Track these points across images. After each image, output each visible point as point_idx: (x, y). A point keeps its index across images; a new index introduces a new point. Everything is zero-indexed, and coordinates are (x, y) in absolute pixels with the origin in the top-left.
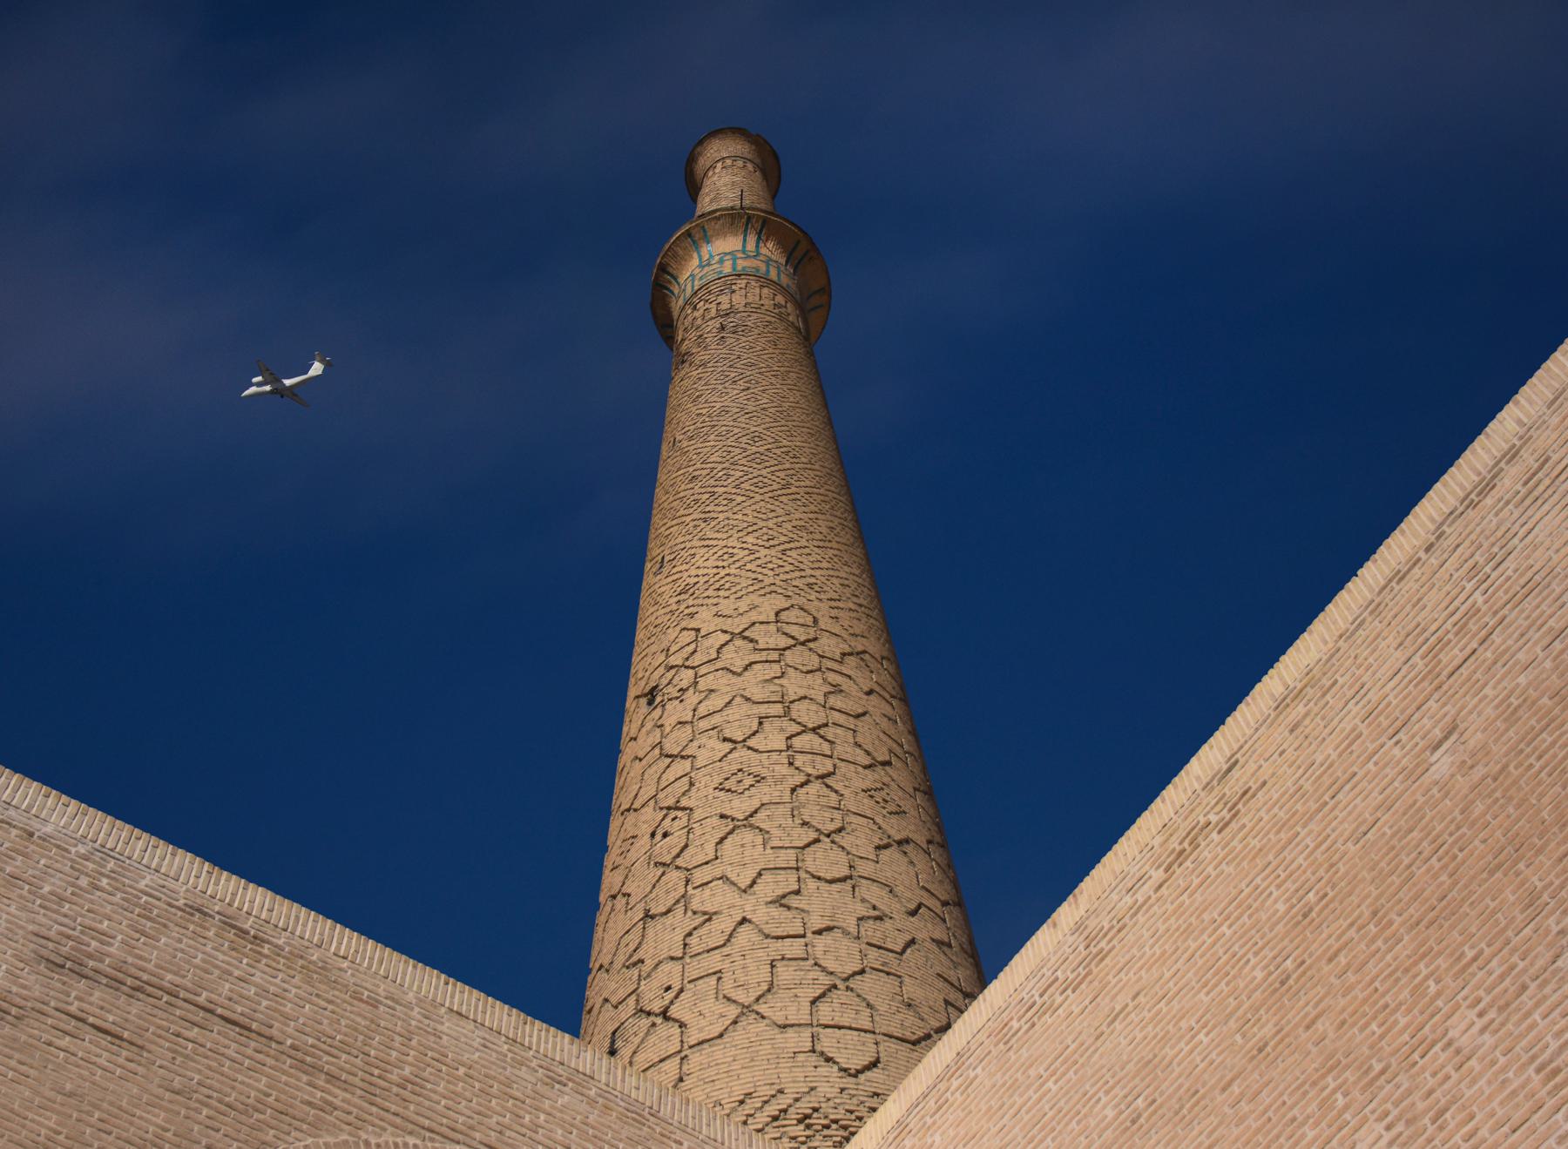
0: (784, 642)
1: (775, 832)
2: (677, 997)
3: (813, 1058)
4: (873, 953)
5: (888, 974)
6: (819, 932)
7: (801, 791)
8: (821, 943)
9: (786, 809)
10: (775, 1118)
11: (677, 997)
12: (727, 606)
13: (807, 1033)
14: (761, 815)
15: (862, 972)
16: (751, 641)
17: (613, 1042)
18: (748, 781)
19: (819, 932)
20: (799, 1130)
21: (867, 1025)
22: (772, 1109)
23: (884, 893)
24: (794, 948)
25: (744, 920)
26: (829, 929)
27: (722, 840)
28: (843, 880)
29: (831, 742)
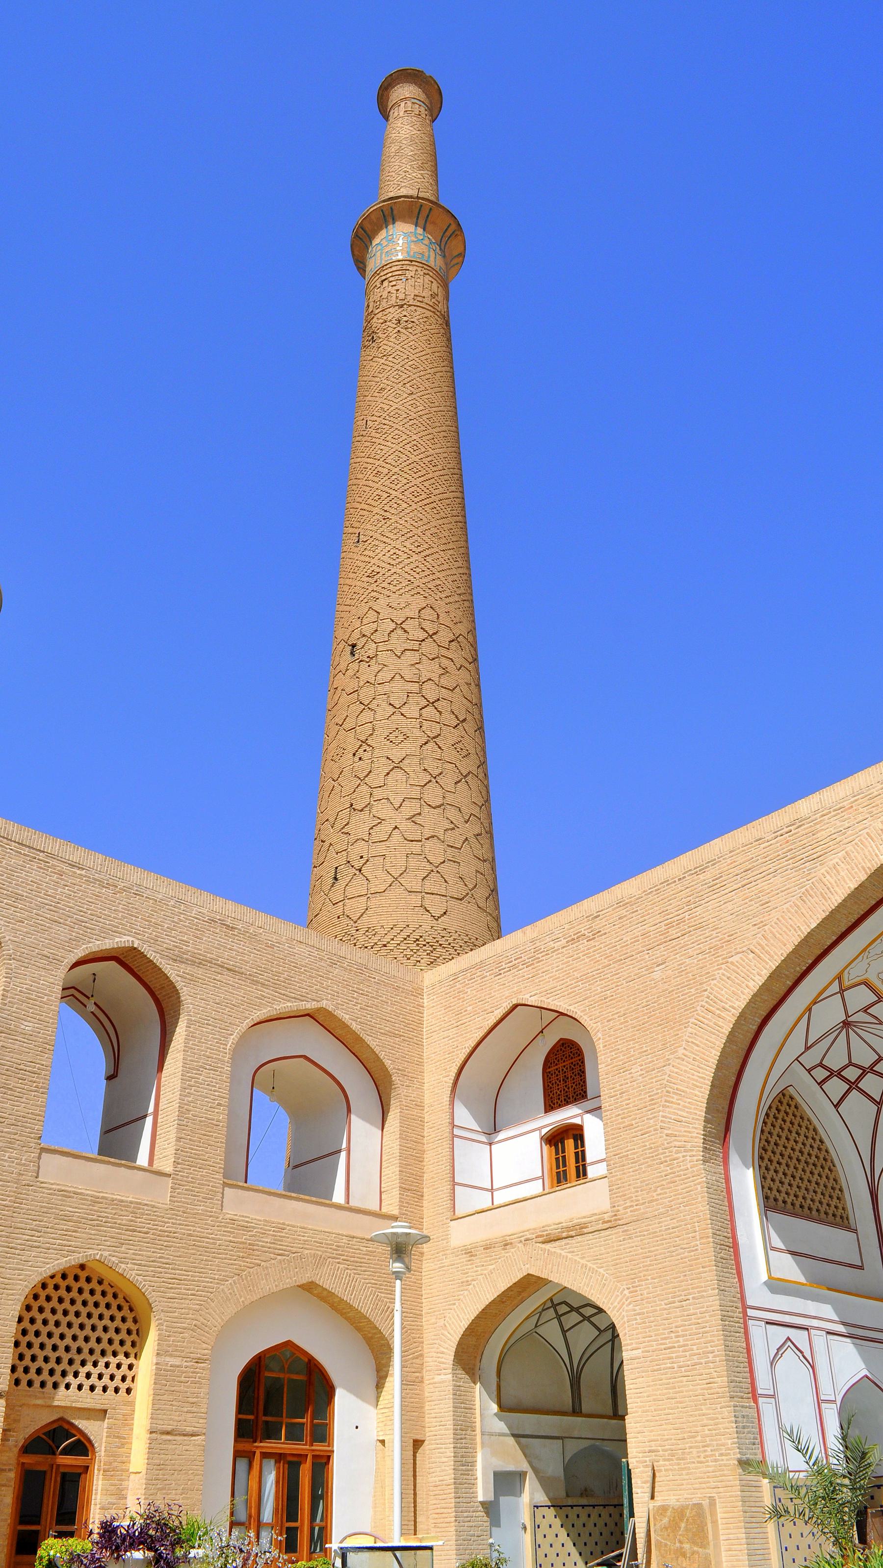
1: (412, 774)
2: (365, 863)
3: (422, 909)
4: (449, 850)
5: (454, 862)
6: (428, 839)
7: (425, 747)
8: (429, 844)
9: (416, 760)
10: (405, 939)
11: (365, 863)
12: (394, 600)
13: (419, 896)
14: (406, 762)
15: (444, 862)
17: (336, 875)
18: (401, 738)
19: (428, 839)
20: (414, 946)
21: (444, 892)
22: (404, 934)
23: (457, 812)
24: (416, 847)
25: (396, 827)
26: (433, 837)
27: (388, 774)
28: (439, 806)
29: (440, 713)
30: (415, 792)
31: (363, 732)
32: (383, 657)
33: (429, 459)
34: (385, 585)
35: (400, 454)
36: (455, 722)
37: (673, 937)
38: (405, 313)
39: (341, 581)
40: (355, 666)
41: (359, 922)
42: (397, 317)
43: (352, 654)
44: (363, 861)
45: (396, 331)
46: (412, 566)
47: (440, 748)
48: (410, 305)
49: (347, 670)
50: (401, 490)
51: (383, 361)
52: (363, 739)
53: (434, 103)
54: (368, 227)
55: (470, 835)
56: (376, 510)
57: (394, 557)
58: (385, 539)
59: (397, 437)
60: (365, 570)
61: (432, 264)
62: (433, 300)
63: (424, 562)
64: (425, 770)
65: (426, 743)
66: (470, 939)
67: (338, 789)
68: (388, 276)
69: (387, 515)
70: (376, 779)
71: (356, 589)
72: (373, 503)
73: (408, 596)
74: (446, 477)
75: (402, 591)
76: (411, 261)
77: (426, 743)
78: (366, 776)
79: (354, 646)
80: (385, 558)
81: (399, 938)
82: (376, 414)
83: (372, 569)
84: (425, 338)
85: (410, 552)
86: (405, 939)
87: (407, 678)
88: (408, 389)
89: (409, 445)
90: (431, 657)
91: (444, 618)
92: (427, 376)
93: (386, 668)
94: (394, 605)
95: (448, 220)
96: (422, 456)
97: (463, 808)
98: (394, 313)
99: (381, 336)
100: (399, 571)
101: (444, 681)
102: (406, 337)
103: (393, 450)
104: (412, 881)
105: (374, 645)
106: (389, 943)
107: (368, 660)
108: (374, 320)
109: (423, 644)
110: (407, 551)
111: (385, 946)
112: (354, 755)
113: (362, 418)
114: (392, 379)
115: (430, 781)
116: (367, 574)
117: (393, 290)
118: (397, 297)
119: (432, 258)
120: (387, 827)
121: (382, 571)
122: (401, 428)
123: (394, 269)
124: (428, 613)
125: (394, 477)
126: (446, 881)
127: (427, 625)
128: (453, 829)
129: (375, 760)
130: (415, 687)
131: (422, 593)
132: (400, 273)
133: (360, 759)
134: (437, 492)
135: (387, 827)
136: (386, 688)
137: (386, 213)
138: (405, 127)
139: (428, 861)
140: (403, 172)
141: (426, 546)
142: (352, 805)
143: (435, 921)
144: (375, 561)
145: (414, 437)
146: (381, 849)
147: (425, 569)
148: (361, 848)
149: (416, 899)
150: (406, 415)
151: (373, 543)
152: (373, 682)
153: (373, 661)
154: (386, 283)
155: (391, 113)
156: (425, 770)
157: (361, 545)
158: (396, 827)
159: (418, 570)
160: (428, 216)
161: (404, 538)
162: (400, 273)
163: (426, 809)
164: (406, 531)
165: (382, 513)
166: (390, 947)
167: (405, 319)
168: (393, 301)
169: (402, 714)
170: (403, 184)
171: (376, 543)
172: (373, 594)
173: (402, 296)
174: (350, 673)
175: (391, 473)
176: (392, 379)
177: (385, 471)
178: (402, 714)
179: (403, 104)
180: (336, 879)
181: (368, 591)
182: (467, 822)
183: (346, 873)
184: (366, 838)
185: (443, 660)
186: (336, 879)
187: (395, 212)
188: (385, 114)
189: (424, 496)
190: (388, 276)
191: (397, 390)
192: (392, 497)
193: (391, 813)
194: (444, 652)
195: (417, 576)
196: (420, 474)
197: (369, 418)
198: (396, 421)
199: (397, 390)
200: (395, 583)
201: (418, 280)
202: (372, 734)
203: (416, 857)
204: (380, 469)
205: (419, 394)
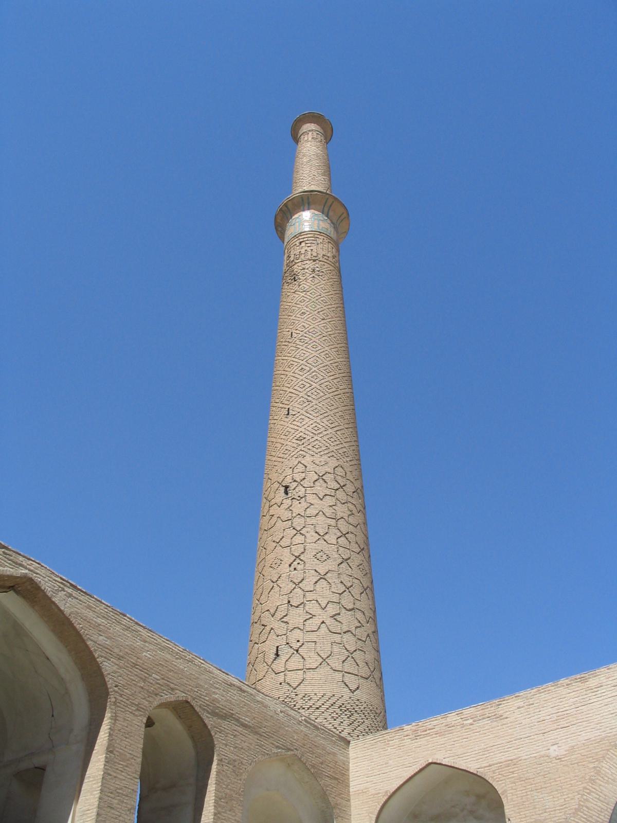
1: (333, 585)
4: (359, 642)
6: (345, 633)
8: (346, 636)
9: (335, 574)
10: (332, 705)
12: (317, 459)
16: (325, 482)
20: (338, 711)
22: (331, 701)
24: (337, 638)
25: (323, 622)
27: (316, 582)
30: (335, 598)
31: (297, 550)
32: (310, 498)
33: (336, 364)
34: (309, 447)
35: (317, 359)
36: (358, 550)
37: (564, 726)
39: (269, 439)
40: (289, 502)
41: (297, 689)
43: (286, 493)
44: (299, 644)
45: (311, 276)
47: (350, 567)
48: (320, 261)
49: (282, 503)
50: (319, 383)
51: (303, 295)
52: (297, 554)
53: (328, 134)
54: (290, 206)
55: (370, 632)
56: (301, 395)
57: (316, 428)
58: (308, 415)
59: (315, 347)
60: (294, 435)
61: (332, 235)
62: (334, 260)
63: (336, 435)
64: (342, 582)
65: (342, 563)
66: (373, 708)
67: (276, 589)
68: (305, 239)
69: (310, 399)
70: (307, 585)
71: (287, 447)
72: (299, 389)
73: (326, 457)
74: (338, 380)
75: (322, 453)
76: (321, 233)
77: (342, 563)
78: (301, 582)
79: (287, 487)
80: (309, 429)
81: (328, 704)
82: (300, 329)
83: (300, 435)
84: (331, 283)
85: (327, 427)
86: (332, 705)
87: (327, 515)
88: (321, 316)
89: (324, 353)
90: (343, 502)
91: (349, 476)
92: (333, 309)
93: (312, 506)
95: (342, 210)
96: (332, 362)
97: (365, 612)
98: (310, 265)
99: (301, 278)
100: (319, 439)
101: (351, 520)
102: (318, 281)
103: (313, 355)
104: (335, 663)
106: (320, 706)
107: (299, 498)
108: (295, 266)
109: (337, 492)
110: (324, 425)
111: (317, 708)
112: (290, 566)
113: (288, 330)
114: (310, 308)
115: (345, 591)
116: (296, 438)
118: (312, 255)
119: (332, 233)
120: (316, 622)
121: (308, 438)
122: (317, 341)
123: (309, 236)
124: (339, 471)
125: (314, 373)
126: (358, 665)
127: (339, 478)
128: (360, 627)
129: (307, 571)
130: (333, 522)
131: (336, 456)
132: (313, 239)
133: (295, 569)
134: (341, 387)
135: (316, 622)
136: (313, 521)
138: (310, 147)
139: (346, 649)
140: (309, 175)
141: (337, 424)
142: (289, 602)
143: (351, 694)
144: (302, 429)
145: (327, 348)
146: (313, 637)
147: (336, 439)
148: (297, 634)
149: (338, 676)
151: (300, 417)
152: (303, 515)
154: (303, 244)
155: (302, 137)
156: (342, 582)
157: (290, 417)
159: (332, 440)
160: (331, 206)
161: (322, 417)
162: (313, 239)
163: (344, 611)
165: (306, 397)
166: (322, 709)
167: (318, 269)
168: (309, 257)
169: (325, 541)
170: (312, 183)
171: (303, 417)
172: (301, 452)
173: (315, 254)
174: (285, 506)
175: (312, 371)
176: (310, 308)
177: (308, 369)
178: (325, 541)
179: (310, 133)
180: (277, 655)
182: (368, 623)
183: (285, 652)
184: (302, 628)
185: (349, 505)
186: (277, 655)
187: (310, 200)
188: (296, 139)
189: (334, 389)
190: (305, 239)
191: (307, 315)
193: (320, 611)
194: (350, 499)
196: (331, 374)
197: (294, 331)
198: (314, 336)
199: (307, 315)
200: (317, 447)
201: (325, 245)
202: (303, 553)
203: (338, 645)
204: (303, 366)
205: (328, 320)
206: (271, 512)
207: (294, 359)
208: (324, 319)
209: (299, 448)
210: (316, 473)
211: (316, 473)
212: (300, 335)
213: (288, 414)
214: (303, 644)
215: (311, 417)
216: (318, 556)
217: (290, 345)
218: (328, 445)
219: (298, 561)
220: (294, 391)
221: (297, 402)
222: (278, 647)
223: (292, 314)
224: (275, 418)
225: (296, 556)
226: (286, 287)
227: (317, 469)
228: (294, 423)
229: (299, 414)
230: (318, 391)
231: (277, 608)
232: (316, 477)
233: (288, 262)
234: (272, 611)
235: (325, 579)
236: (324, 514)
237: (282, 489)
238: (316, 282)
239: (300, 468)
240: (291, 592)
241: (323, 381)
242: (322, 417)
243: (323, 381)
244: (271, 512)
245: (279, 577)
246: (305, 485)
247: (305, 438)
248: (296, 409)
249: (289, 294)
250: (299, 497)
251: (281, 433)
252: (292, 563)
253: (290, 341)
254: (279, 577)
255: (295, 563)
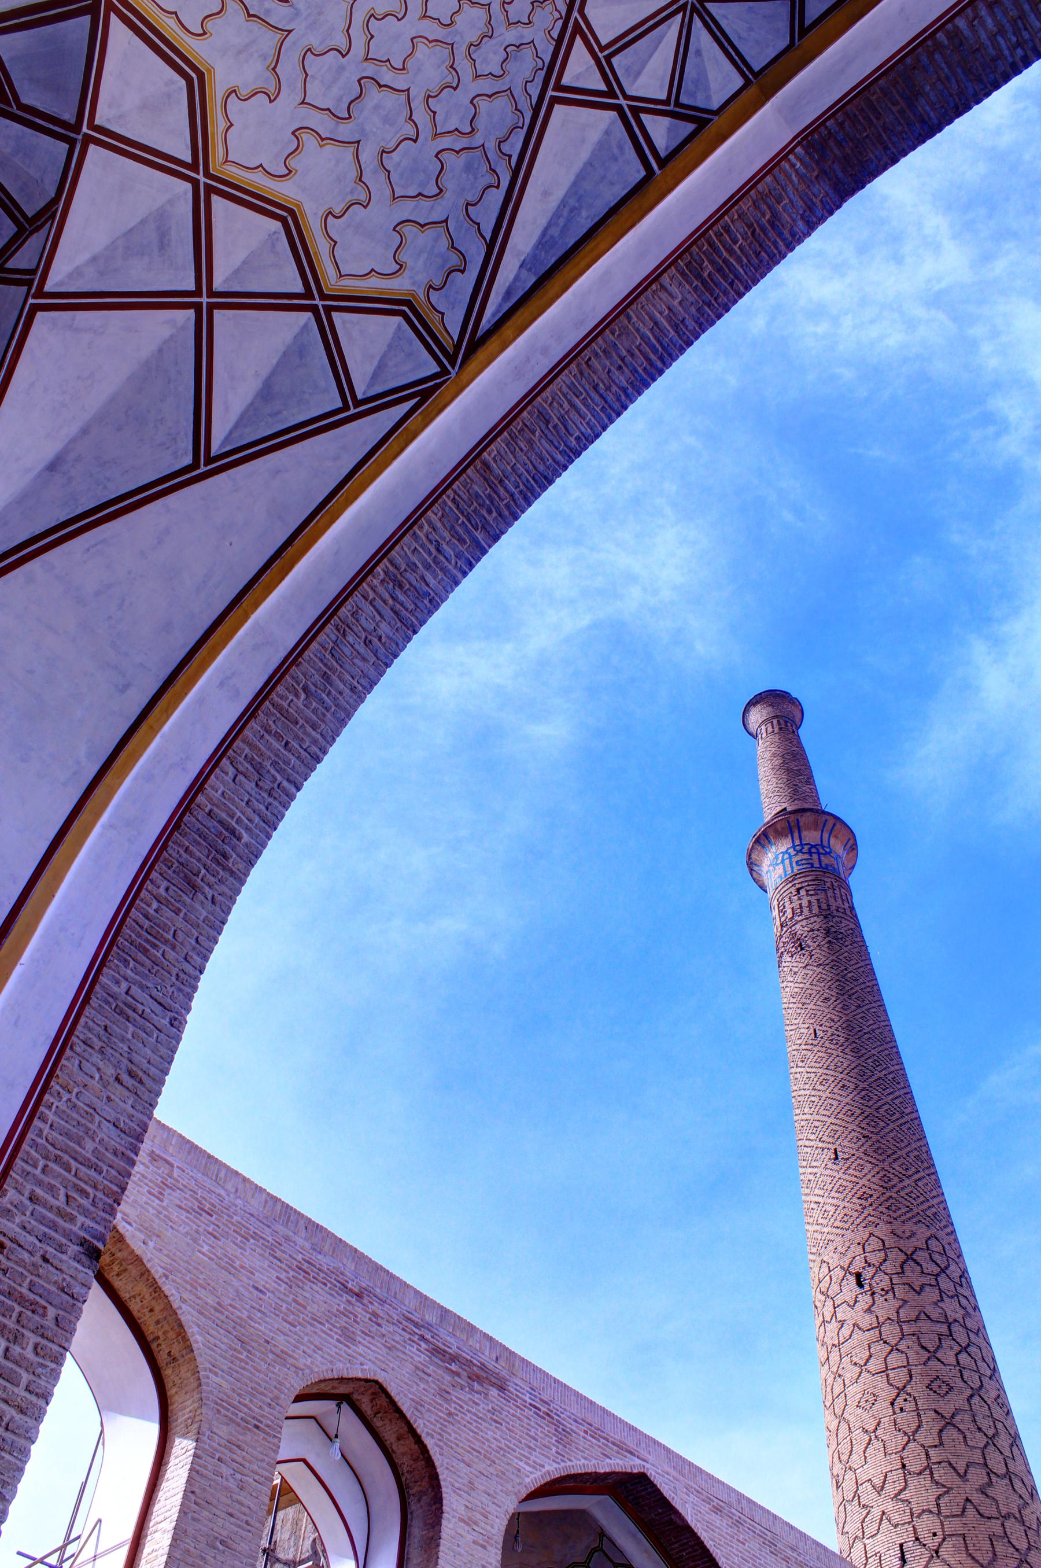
0: (936, 1270)
14: (958, 1418)
18: (945, 1388)
25: (967, 1500)
38: (831, 923)
42: (824, 926)
43: (860, 1284)
44: (938, 1539)
46: (907, 1190)
49: (856, 1302)
58: (870, 1159)
60: (853, 1191)
73: (910, 1223)
94: (899, 1233)
96: (885, 1072)
100: (895, 1195)
105: (887, 1277)
107: (883, 1293)
112: (892, 1404)
113: (806, 1026)
117: (813, 899)
133: (901, 1409)
137: (792, 824)
142: (904, 1466)
145: (873, 1052)
150: (858, 1029)
153: (890, 1295)
154: (803, 892)
158: (967, 1500)
161: (890, 1160)
164: (891, 1152)
167: (833, 929)
171: (862, 1162)
172: (870, 1218)
178: (939, 1360)
181: (863, 1215)
185: (962, 1299)
187: (801, 824)
189: (898, 1115)
192: (866, 1114)
193: (957, 1481)
195: (913, 1201)
196: (889, 1091)
197: (817, 1028)
202: (909, 1382)
204: (845, 1083)
206: (840, 1316)
207: (828, 1072)
208: (859, 1006)
209: (866, 1212)
210: (901, 1250)
211: (901, 1250)
212: (829, 1034)
213: (836, 1158)
214: (944, 1540)
215: (874, 1161)
216: (934, 1386)
217: (816, 1049)
218: (909, 1204)
219: (903, 1396)
220: (838, 1122)
221: (849, 1139)
222: (901, 1545)
223: (808, 1001)
224: (814, 1164)
225: (898, 1388)
226: (789, 959)
227: (902, 1244)
228: (849, 1172)
229: (854, 1158)
230: (876, 1120)
231: (886, 1476)
232: (903, 1257)
233: (783, 919)
234: (878, 1482)
235: (954, 1425)
236: (928, 1316)
237: (852, 1280)
238: (835, 950)
239: (875, 1244)
240: (904, 1449)
241: (879, 1104)
242: (890, 1160)
243: (879, 1104)
244: (840, 1316)
245: (878, 1424)
246: (889, 1271)
247: (871, 1196)
248: (846, 1150)
249: (796, 970)
250: (883, 1290)
251: (830, 1188)
252: (895, 1400)
253: (815, 1042)
254: (878, 1424)
255: (900, 1400)
